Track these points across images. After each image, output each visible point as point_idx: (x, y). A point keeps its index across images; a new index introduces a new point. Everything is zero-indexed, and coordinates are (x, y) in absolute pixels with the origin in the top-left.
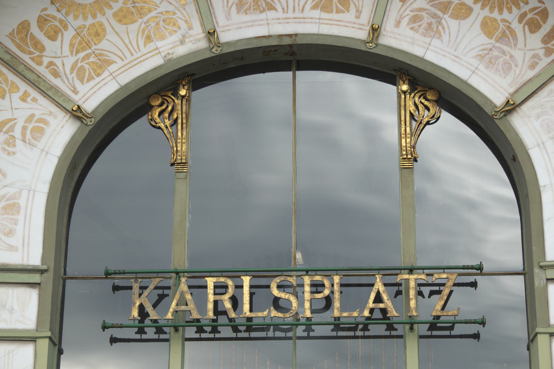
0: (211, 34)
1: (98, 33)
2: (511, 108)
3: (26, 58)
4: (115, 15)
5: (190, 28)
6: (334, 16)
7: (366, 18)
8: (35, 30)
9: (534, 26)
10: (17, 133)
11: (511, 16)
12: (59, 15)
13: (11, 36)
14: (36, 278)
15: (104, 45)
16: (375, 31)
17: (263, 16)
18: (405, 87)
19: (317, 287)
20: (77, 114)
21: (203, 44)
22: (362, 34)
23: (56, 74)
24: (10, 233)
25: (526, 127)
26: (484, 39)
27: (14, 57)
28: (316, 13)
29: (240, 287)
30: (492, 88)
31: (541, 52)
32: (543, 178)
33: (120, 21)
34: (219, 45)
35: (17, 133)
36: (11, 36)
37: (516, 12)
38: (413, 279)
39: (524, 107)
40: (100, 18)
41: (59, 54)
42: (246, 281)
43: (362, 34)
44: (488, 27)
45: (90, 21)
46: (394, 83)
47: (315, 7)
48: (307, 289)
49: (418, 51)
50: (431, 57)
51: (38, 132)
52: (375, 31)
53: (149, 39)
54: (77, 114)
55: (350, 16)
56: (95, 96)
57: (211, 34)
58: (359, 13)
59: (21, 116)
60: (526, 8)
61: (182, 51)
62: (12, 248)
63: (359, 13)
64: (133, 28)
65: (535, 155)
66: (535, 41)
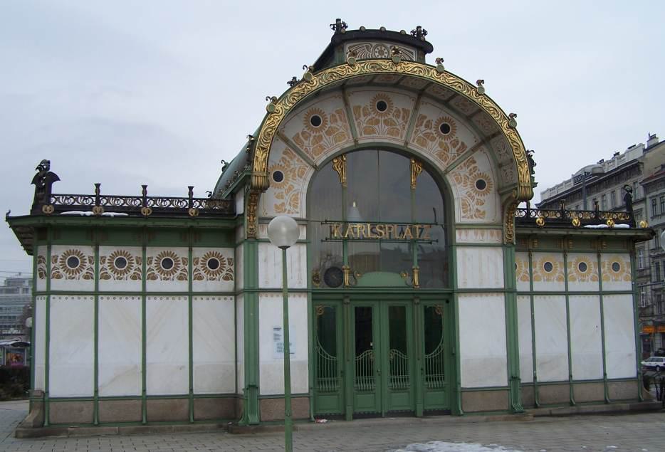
0: (356, 141)
1: (320, 138)
2: (447, 172)
3: (298, 146)
4: (326, 132)
5: (349, 138)
6: (394, 137)
7: (403, 138)
8: (301, 136)
9: (455, 146)
10: (296, 172)
11: (448, 142)
12: (308, 131)
13: (293, 138)
14: (305, 223)
15: (322, 142)
16: (406, 143)
17: (372, 135)
18: (413, 162)
19: (390, 228)
20: (315, 167)
21: (353, 144)
22: (403, 144)
23: (307, 152)
24: (296, 207)
25: (450, 179)
26: (439, 149)
27: (296, 147)
28: (388, 136)
29: (367, 227)
30: (441, 165)
31: (456, 155)
32: (455, 196)
33: (327, 134)
34: (358, 145)
35: (296, 172)
36: (293, 138)
37: (449, 141)
38: (417, 226)
39: (450, 172)
40: (321, 133)
41: (308, 144)
42: (369, 225)
43: (403, 144)
44: (441, 144)
45: (318, 134)
46: (409, 158)
47: (388, 134)
48: (387, 229)
49: (419, 151)
50: (423, 153)
51: (303, 173)
52: (406, 143)
53: (336, 142)
54: (315, 167)
55: (399, 137)
56: (319, 160)
57: (356, 141)
58: (401, 137)
59: (297, 166)
60: (452, 139)
61: (346, 146)
62: (298, 213)
63: (401, 137)
64: (331, 137)
65: (453, 188)
66: (454, 150)
